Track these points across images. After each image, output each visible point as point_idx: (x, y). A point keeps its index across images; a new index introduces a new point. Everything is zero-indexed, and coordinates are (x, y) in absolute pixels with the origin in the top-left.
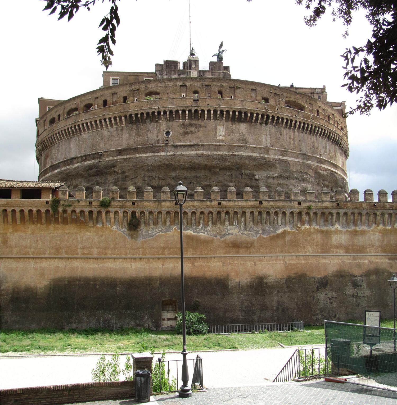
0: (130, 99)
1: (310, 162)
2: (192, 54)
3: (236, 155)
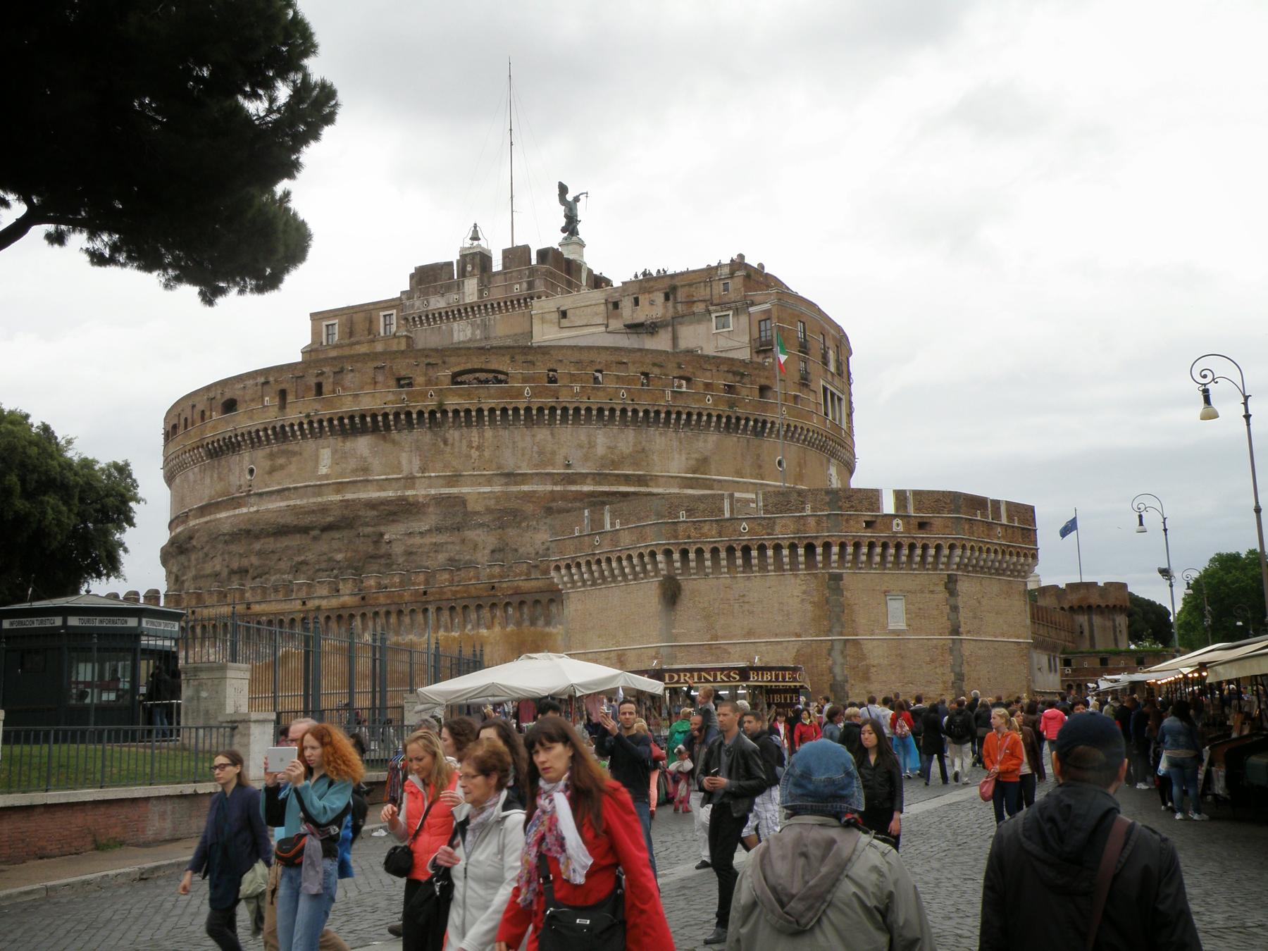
0: (207, 414)
1: (525, 488)
2: (475, 237)
3: (348, 501)
